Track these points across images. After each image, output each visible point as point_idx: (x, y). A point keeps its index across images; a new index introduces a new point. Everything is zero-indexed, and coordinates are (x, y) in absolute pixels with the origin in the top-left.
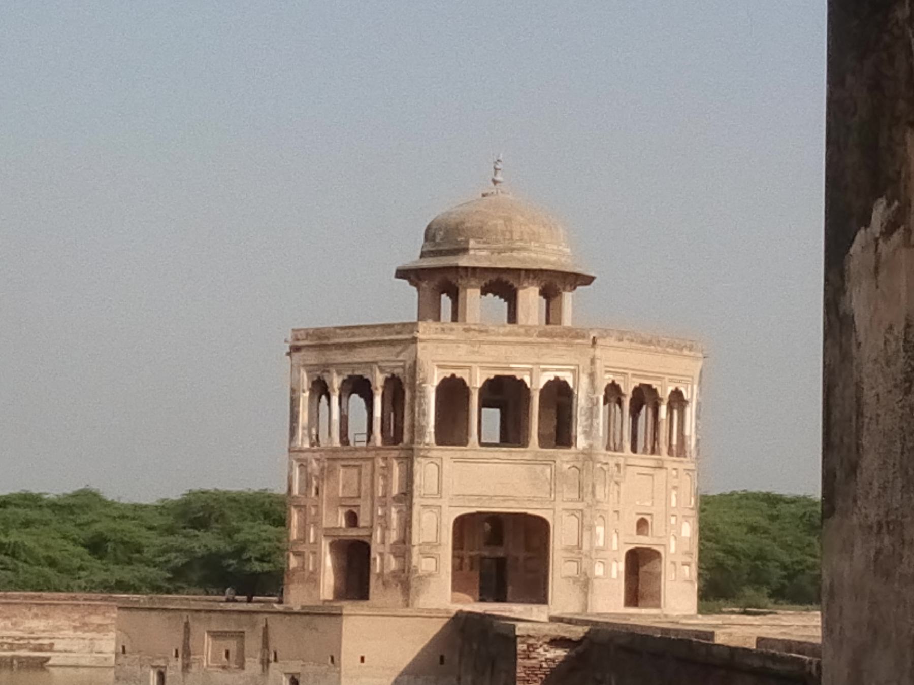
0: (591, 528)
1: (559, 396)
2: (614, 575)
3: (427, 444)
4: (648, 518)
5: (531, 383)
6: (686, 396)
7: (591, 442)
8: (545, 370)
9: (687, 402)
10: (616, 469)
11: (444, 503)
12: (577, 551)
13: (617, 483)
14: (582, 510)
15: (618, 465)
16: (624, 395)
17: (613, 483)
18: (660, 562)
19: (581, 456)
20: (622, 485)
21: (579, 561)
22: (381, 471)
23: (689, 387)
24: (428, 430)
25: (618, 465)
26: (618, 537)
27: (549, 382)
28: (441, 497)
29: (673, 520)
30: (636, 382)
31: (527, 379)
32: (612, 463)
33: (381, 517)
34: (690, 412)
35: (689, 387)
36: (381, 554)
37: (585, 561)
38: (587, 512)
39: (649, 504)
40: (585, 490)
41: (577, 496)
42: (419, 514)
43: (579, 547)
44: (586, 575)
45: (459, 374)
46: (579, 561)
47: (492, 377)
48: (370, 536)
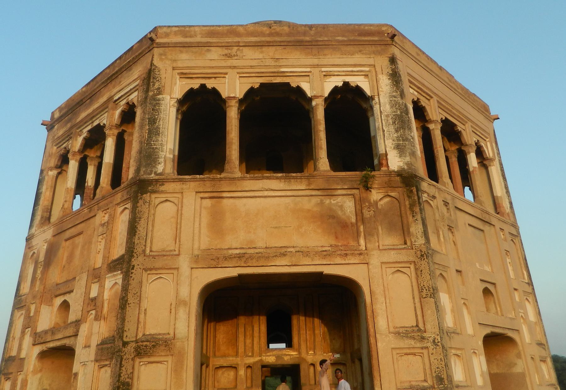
0: (434, 293)
1: (350, 107)
2: (480, 381)
3: (161, 174)
4: (491, 288)
5: (312, 88)
6: (489, 151)
7: (408, 159)
8: (328, 75)
9: (491, 160)
10: (444, 209)
11: (184, 263)
13: (450, 228)
18: (519, 356)
20: (456, 233)
22: (101, 229)
23: (489, 144)
24: (162, 154)
25: (446, 204)
27: (336, 88)
28: (179, 255)
29: (516, 295)
30: (444, 115)
31: (306, 87)
33: (94, 300)
34: (494, 170)
35: (489, 144)
36: (84, 364)
39: (488, 269)
42: (141, 283)
45: (210, 84)
47: (257, 86)
48: (76, 335)
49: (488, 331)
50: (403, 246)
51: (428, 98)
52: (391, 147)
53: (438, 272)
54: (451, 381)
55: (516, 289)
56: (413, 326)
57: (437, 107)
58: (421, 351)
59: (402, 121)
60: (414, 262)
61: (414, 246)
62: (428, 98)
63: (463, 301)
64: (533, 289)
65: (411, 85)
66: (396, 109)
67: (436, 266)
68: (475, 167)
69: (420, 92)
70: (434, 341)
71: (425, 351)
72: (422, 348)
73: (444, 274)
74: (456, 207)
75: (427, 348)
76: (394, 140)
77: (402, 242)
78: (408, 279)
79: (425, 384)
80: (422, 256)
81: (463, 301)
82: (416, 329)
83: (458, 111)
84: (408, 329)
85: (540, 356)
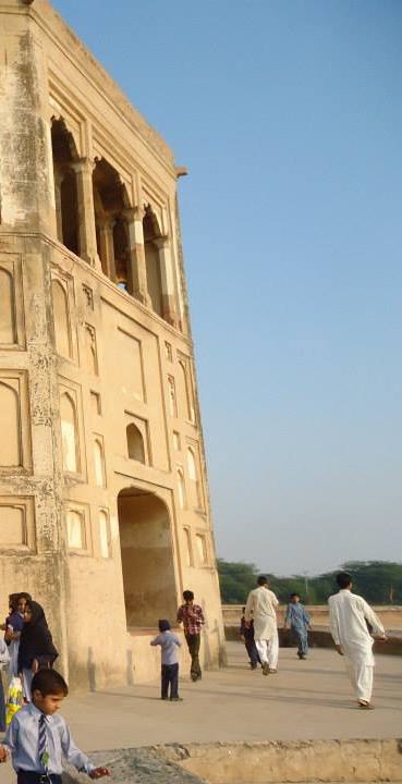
0: (51, 419)
9: (165, 238)
12: (18, 479)
13: (90, 329)
14: (27, 371)
15: (87, 290)
16: (83, 160)
17: (82, 329)
18: (166, 525)
19: (15, 242)
21: (25, 507)
26: (102, 455)
32: (78, 284)
37: (44, 508)
38: (39, 376)
40: (29, 322)
41: (9, 336)
43: (24, 465)
44: (48, 544)
46: (25, 507)
49: (128, 483)
50: (11, 347)
51: (78, 119)
52: (8, 188)
53: (63, 390)
54: (64, 546)
55: (176, 433)
56: (14, 466)
57: (90, 138)
58: (23, 502)
59: (31, 147)
60: (27, 371)
61: (29, 347)
62: (78, 119)
63: (95, 437)
64: (201, 435)
65: (53, 92)
66: (24, 125)
67: (62, 381)
68: (140, 245)
69: (64, 104)
70: (44, 489)
71: (28, 502)
72: (25, 497)
73: (71, 394)
74: (102, 298)
75: (32, 497)
76: (14, 177)
77: (11, 340)
78: (13, 399)
79: (24, 548)
80: (40, 361)
81: (95, 437)
82: (20, 469)
83: (122, 148)
84: (6, 470)
85: (198, 529)
